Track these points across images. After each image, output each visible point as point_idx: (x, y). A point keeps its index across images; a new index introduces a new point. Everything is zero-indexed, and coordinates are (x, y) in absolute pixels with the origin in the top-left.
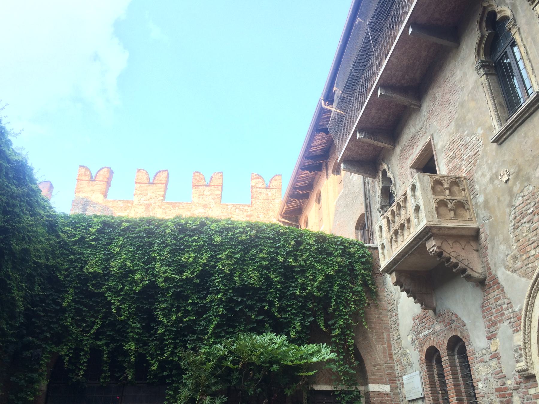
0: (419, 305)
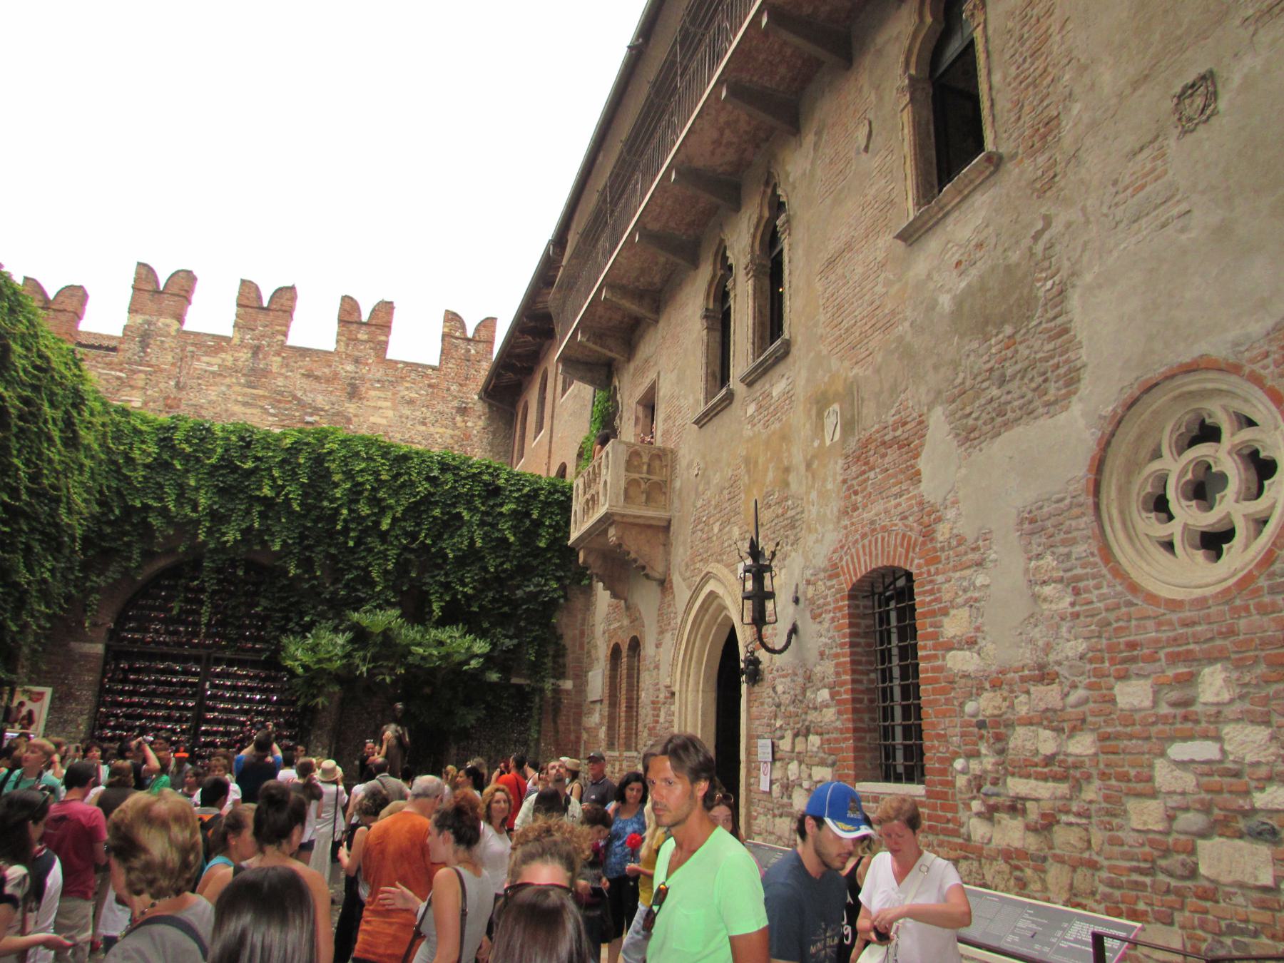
0: (608, 592)
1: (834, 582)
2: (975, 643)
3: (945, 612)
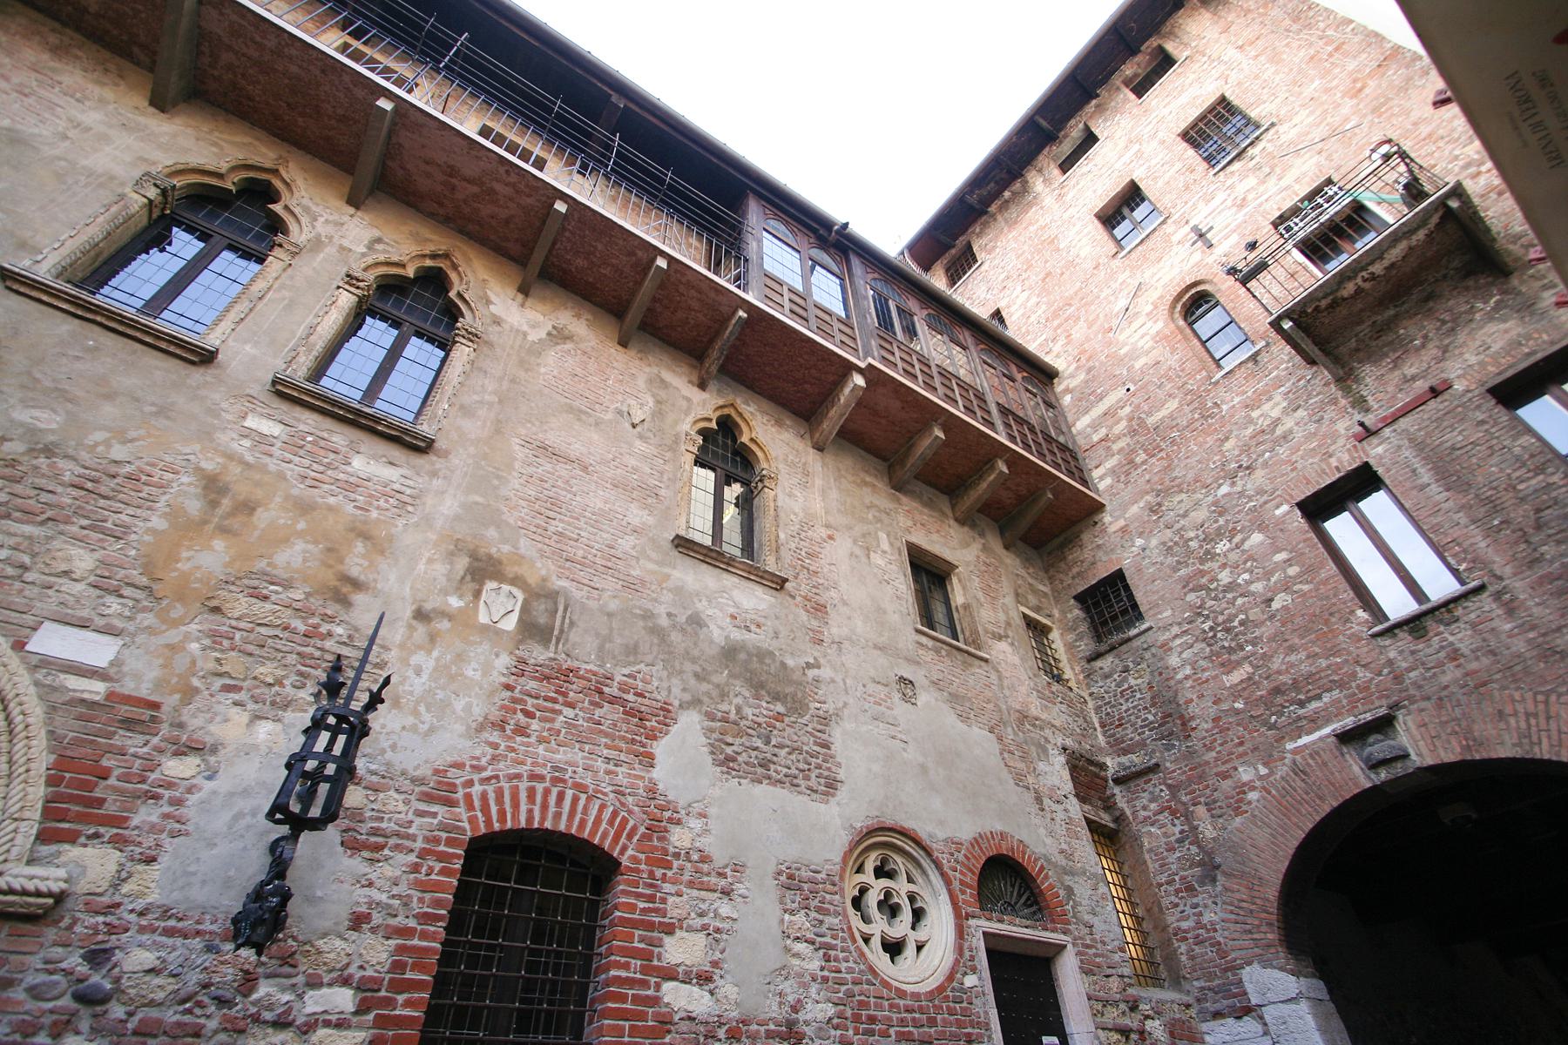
1: (434, 808)
2: (709, 979)
3: (669, 930)
